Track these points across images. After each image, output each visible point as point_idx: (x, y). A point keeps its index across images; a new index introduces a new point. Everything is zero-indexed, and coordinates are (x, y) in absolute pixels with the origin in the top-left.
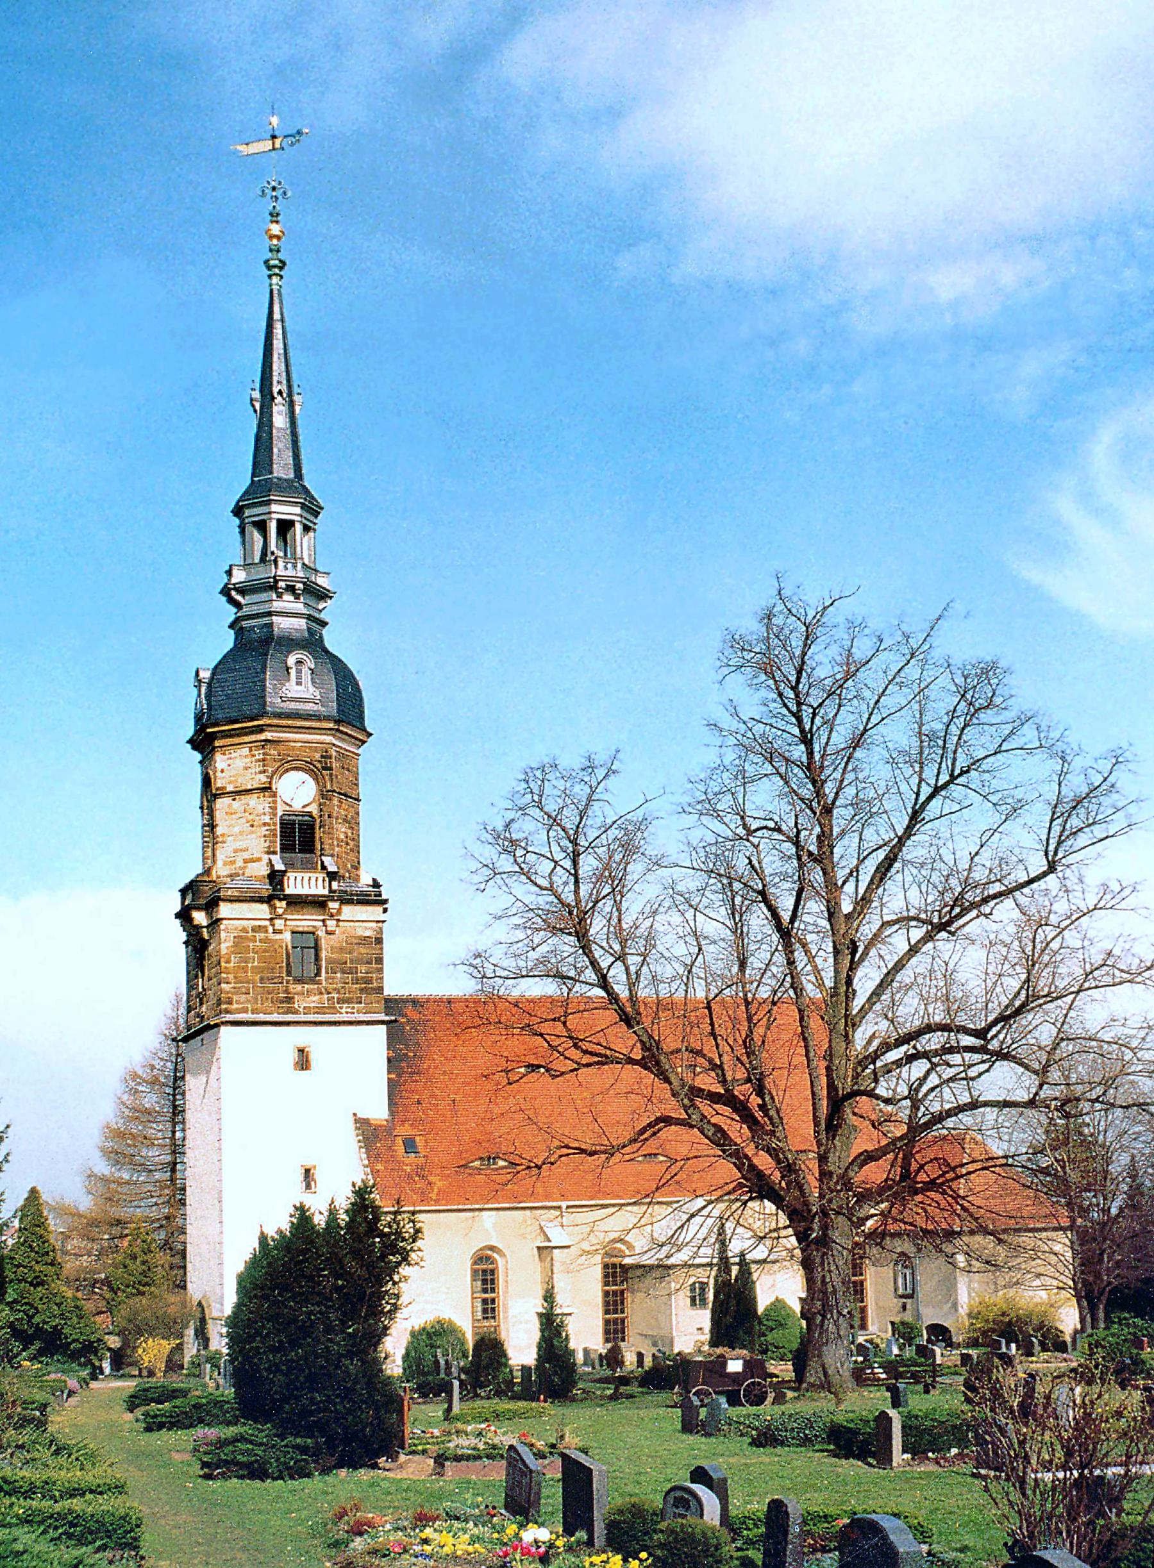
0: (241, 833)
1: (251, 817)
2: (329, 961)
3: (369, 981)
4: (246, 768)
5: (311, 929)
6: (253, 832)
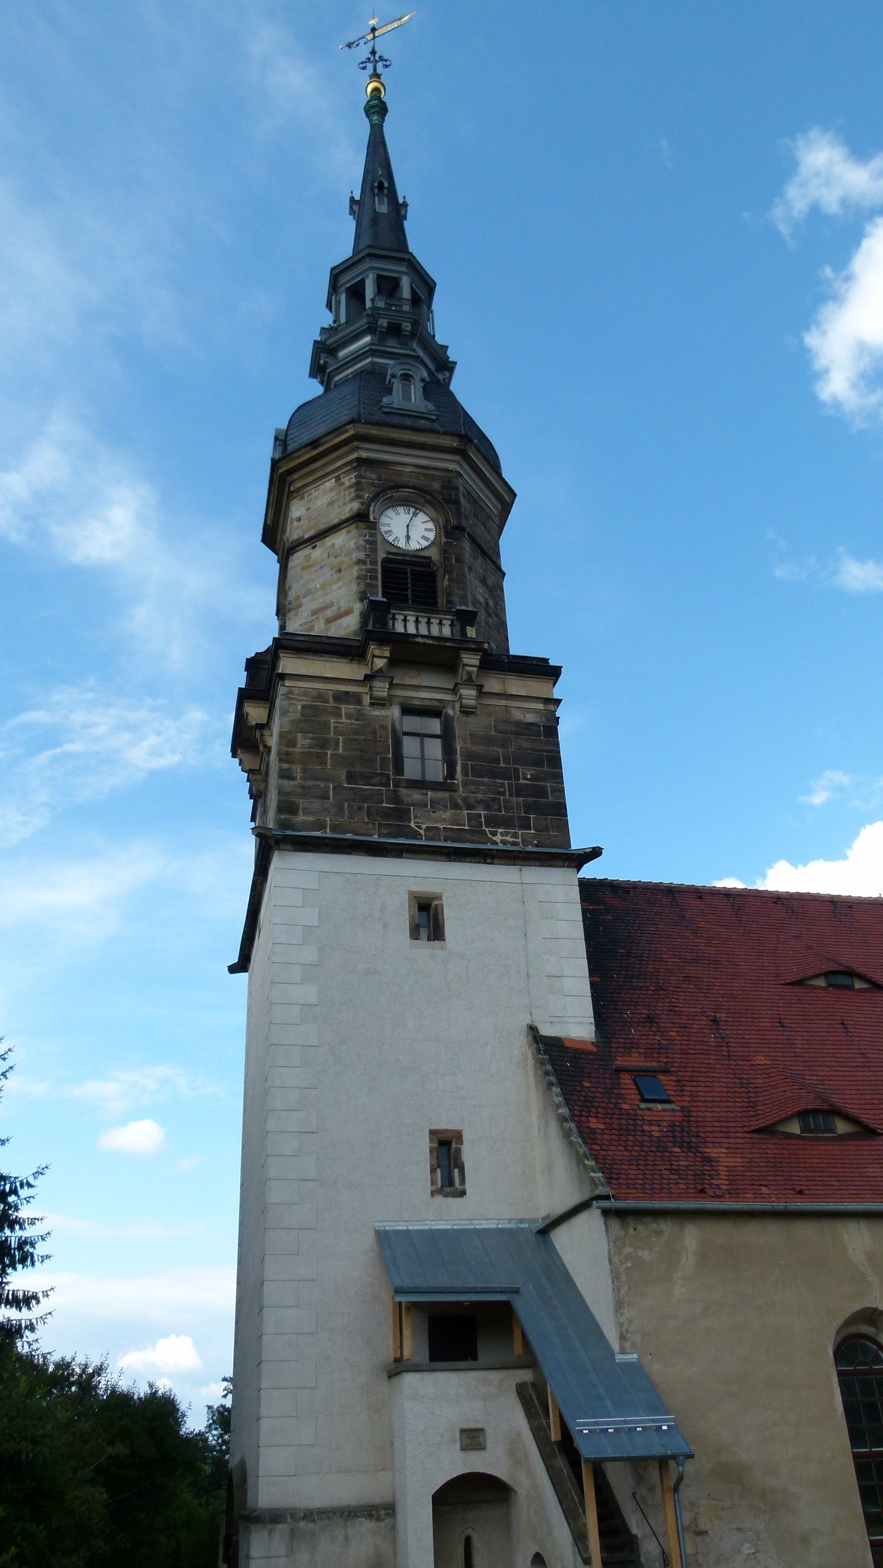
0: (323, 587)
1: (339, 560)
2: (468, 756)
3: (541, 792)
4: (331, 504)
5: (436, 704)
6: (339, 580)
